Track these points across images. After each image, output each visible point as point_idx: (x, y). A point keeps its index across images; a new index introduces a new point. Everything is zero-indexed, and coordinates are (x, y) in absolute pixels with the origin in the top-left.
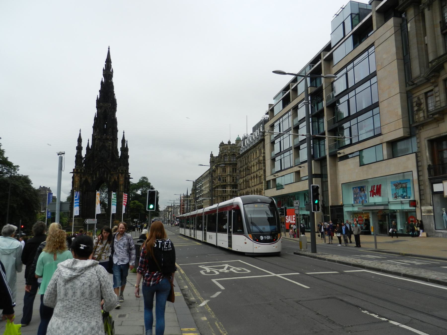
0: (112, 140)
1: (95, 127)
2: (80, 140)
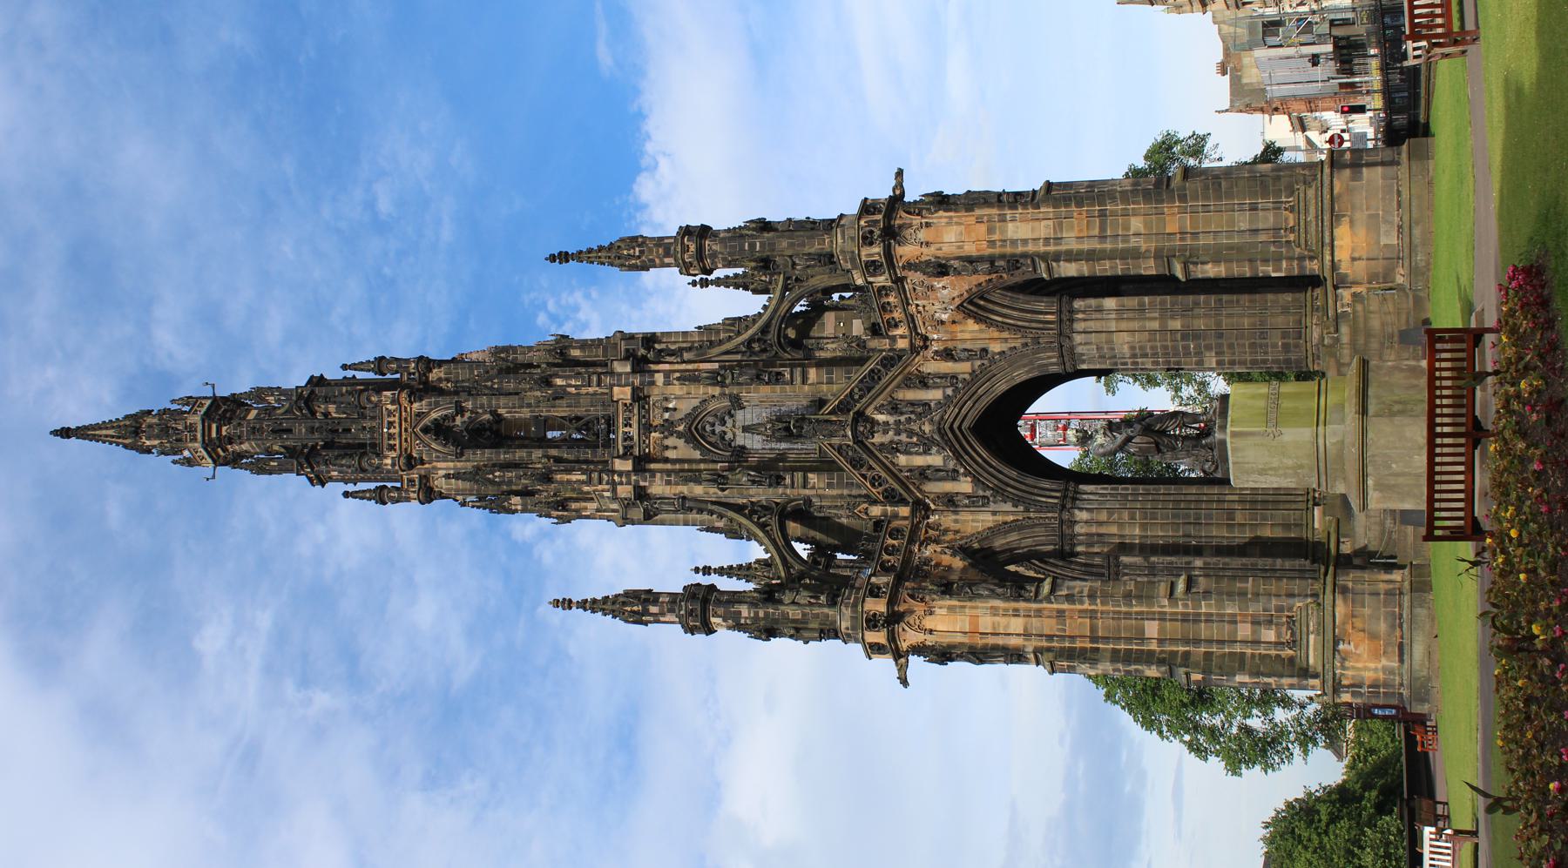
0: (640, 365)
1: (562, 508)
2: (635, 606)
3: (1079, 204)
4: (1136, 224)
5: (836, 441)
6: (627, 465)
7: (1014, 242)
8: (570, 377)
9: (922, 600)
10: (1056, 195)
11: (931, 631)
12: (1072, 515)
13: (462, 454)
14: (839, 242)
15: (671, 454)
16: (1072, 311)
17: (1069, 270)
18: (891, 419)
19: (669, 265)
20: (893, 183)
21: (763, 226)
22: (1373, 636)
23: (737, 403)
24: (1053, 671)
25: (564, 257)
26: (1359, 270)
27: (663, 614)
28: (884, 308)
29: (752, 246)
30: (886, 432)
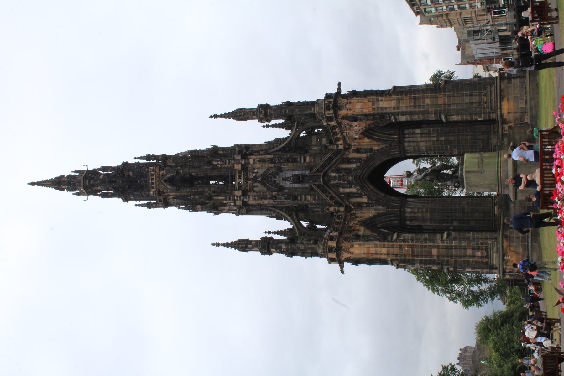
1: (216, 209)
2: (243, 245)
3: (406, 94)
4: (427, 101)
5: (317, 183)
6: (238, 193)
7: (382, 108)
8: (218, 161)
9: (349, 241)
10: (398, 91)
11: (352, 253)
12: (405, 210)
13: (179, 190)
14: (317, 110)
15: (256, 189)
16: (404, 134)
17: (403, 118)
18: (337, 175)
19: (254, 119)
20: (337, 87)
21: (288, 104)
22: (517, 253)
23: (280, 170)
24: (398, 267)
25: (216, 116)
26: (511, 117)
27: (253, 248)
28: (335, 134)
29: (285, 111)
30: (335, 180)
